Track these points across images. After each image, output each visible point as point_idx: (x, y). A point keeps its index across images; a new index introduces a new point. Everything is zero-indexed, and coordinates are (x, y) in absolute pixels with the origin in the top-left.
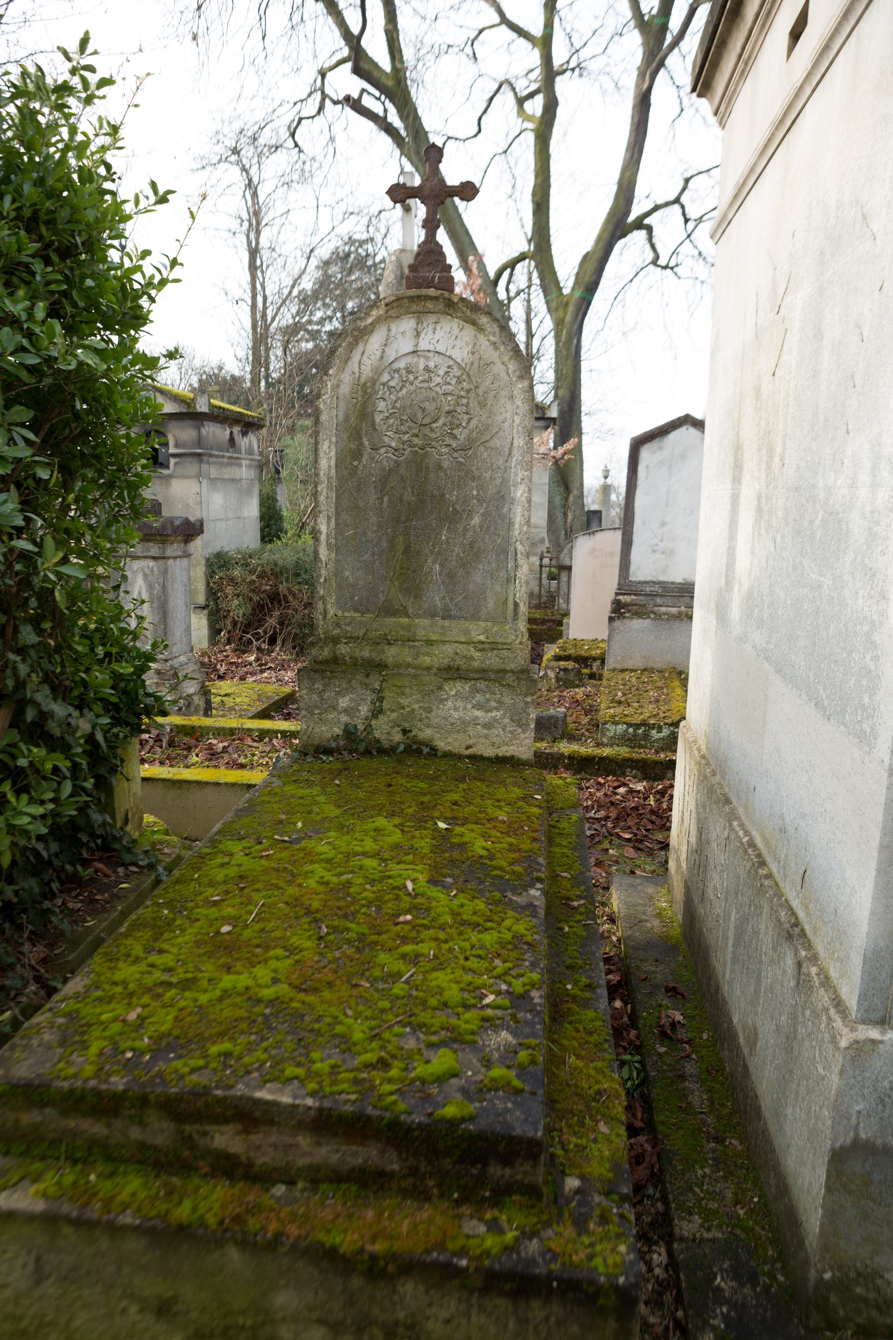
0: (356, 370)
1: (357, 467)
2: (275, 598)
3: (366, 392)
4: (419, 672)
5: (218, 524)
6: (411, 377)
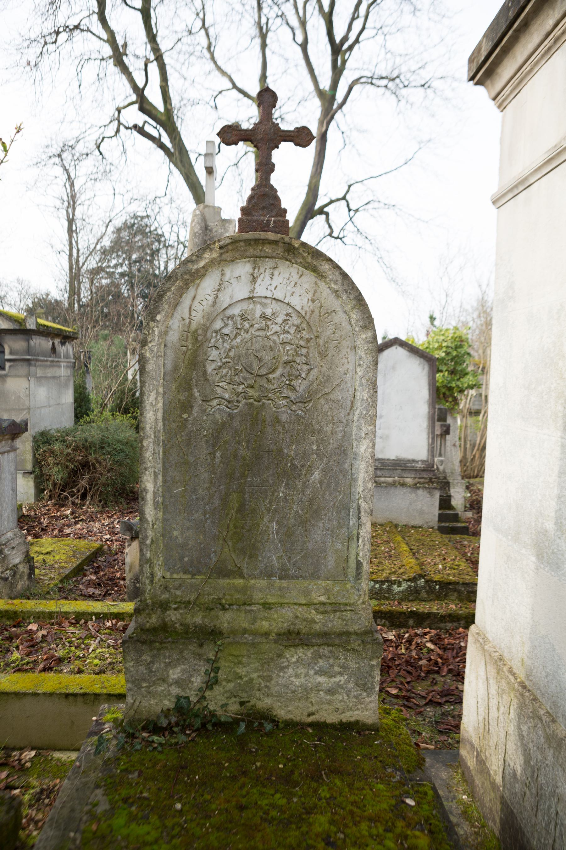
0: (186, 316)
1: (186, 420)
3: (197, 340)
4: (257, 640)
6: (247, 325)
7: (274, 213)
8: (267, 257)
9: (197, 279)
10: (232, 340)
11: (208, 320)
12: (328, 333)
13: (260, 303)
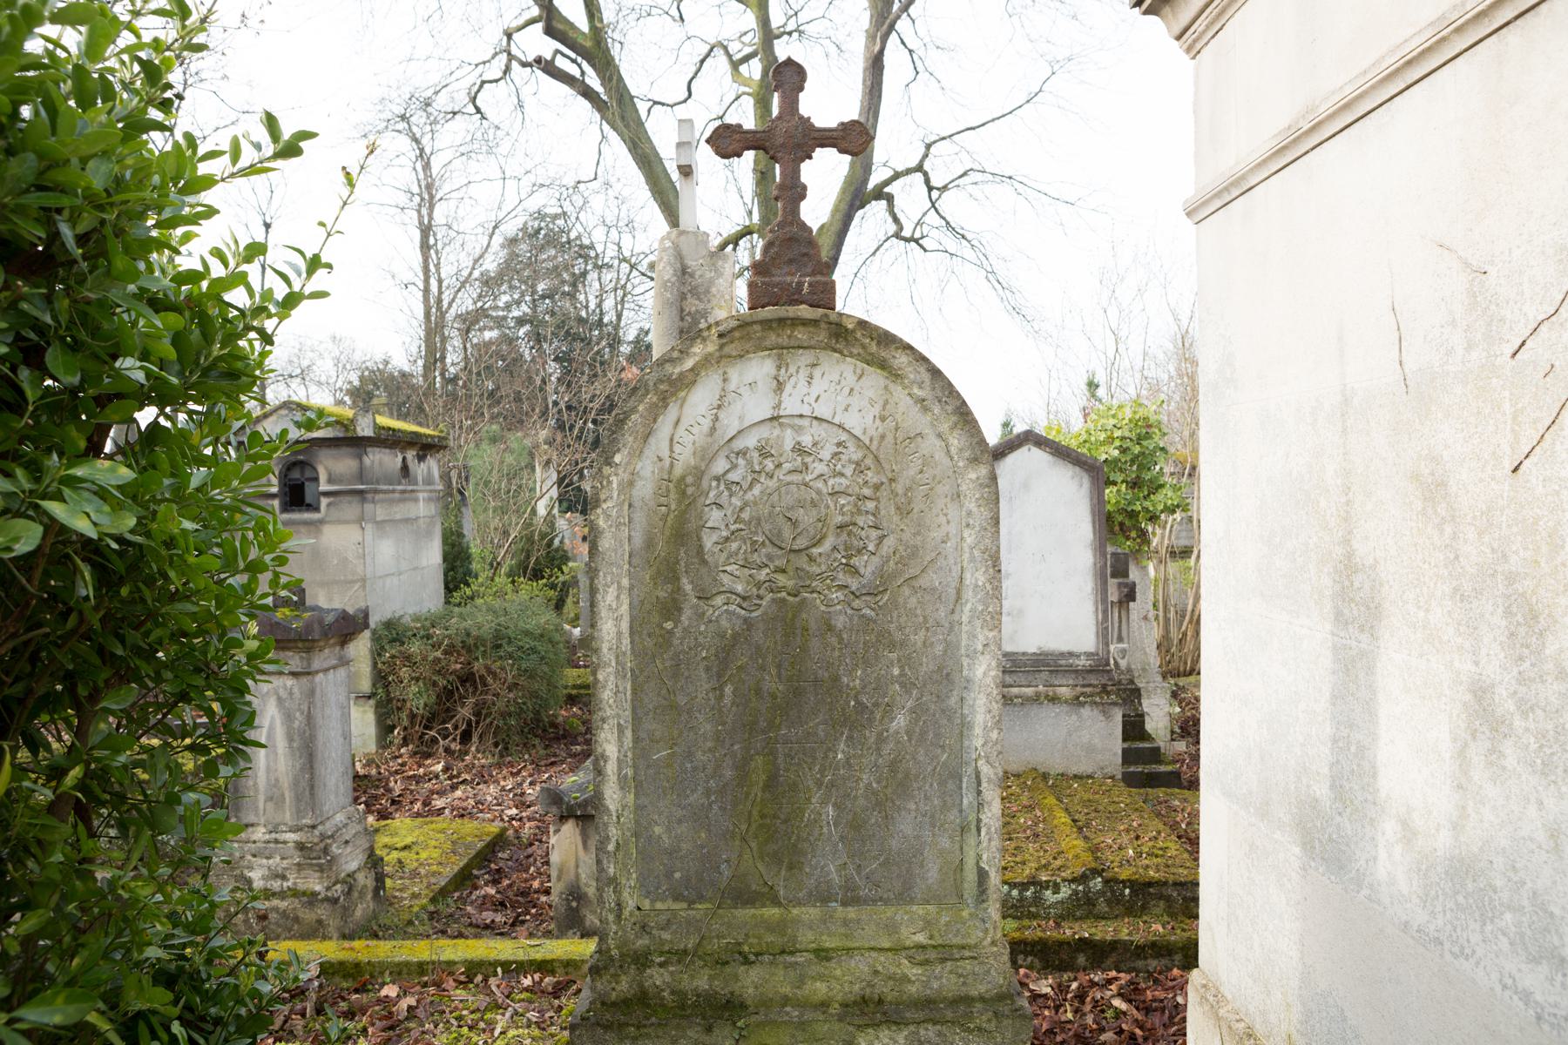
0: (665, 453)
1: (670, 632)
2: (467, 678)
3: (684, 496)
4: (808, 1016)
5: (388, 581)
6: (769, 465)
7: (809, 270)
8: (799, 347)
9: (681, 389)
11: (702, 460)
12: (912, 472)
13: (792, 427)
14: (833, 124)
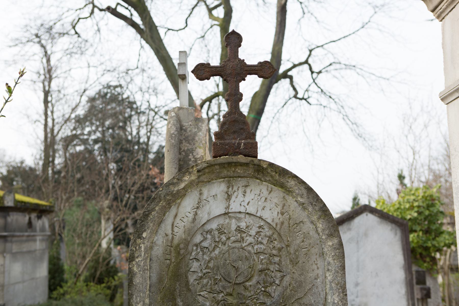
0: (169, 232)
3: (179, 253)
6: (224, 238)
7: (244, 137)
8: (239, 177)
9: (178, 199)
10: (211, 252)
11: (189, 235)
12: (298, 242)
13: (235, 218)
14: (255, 63)
